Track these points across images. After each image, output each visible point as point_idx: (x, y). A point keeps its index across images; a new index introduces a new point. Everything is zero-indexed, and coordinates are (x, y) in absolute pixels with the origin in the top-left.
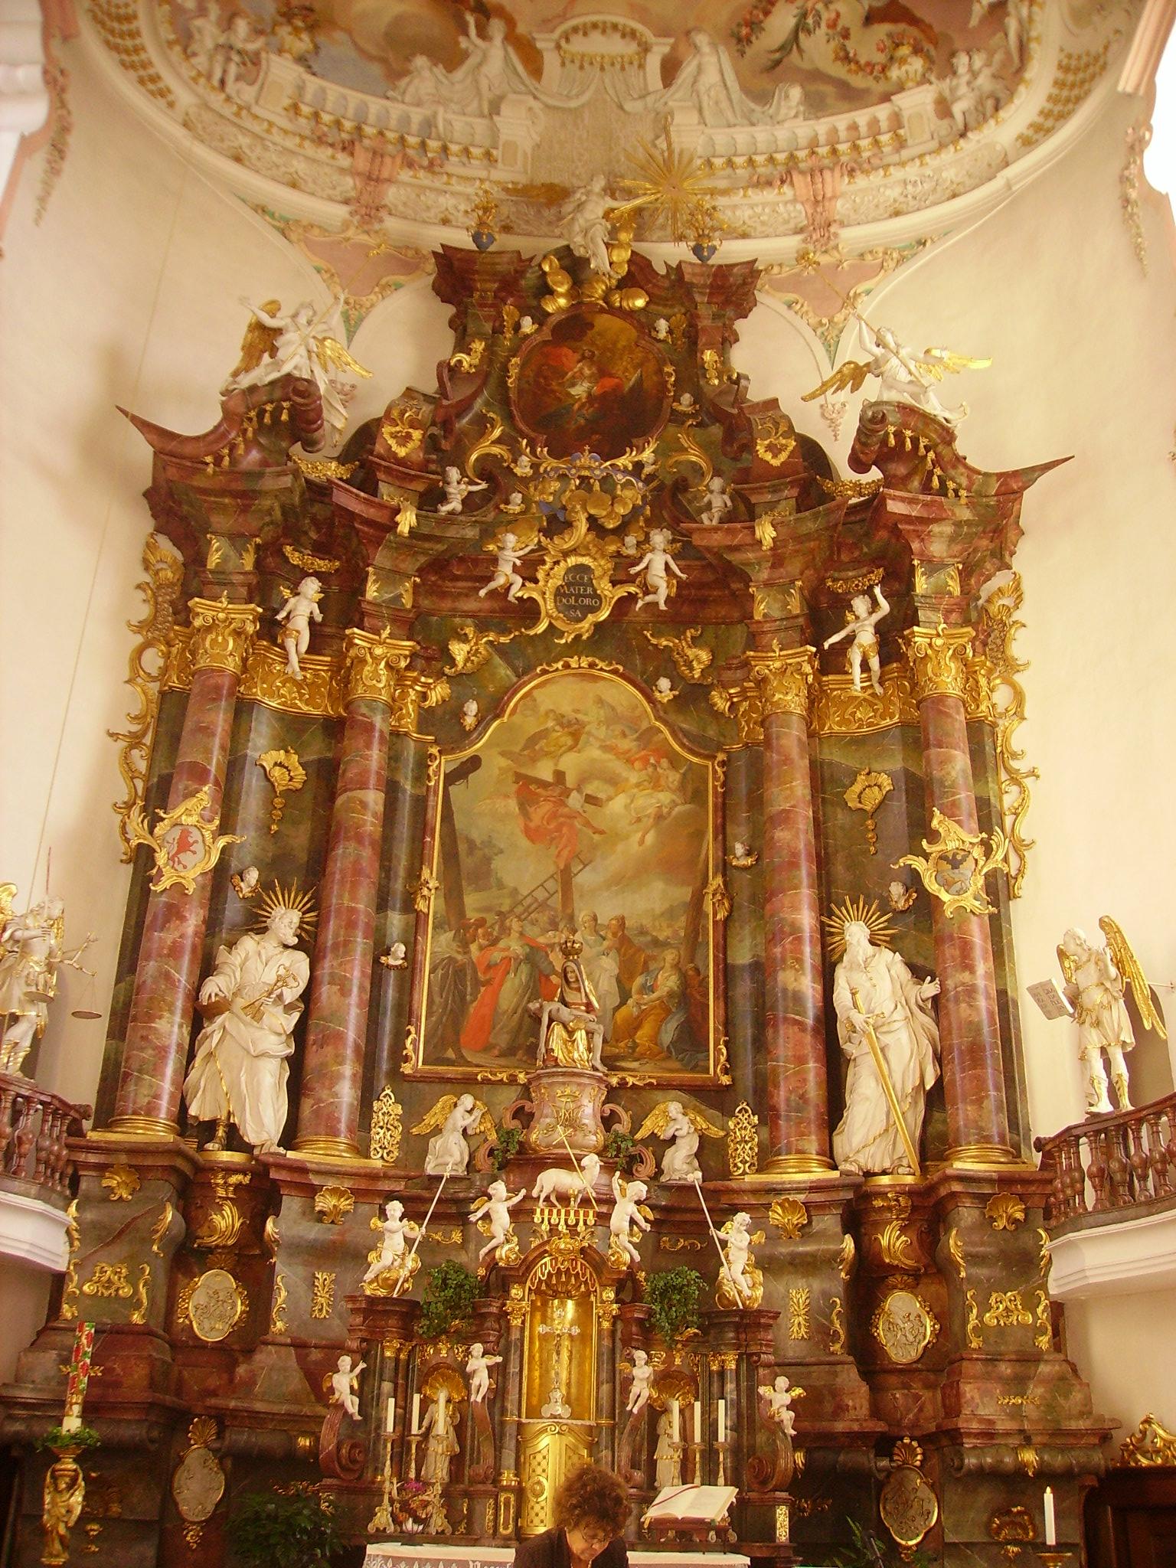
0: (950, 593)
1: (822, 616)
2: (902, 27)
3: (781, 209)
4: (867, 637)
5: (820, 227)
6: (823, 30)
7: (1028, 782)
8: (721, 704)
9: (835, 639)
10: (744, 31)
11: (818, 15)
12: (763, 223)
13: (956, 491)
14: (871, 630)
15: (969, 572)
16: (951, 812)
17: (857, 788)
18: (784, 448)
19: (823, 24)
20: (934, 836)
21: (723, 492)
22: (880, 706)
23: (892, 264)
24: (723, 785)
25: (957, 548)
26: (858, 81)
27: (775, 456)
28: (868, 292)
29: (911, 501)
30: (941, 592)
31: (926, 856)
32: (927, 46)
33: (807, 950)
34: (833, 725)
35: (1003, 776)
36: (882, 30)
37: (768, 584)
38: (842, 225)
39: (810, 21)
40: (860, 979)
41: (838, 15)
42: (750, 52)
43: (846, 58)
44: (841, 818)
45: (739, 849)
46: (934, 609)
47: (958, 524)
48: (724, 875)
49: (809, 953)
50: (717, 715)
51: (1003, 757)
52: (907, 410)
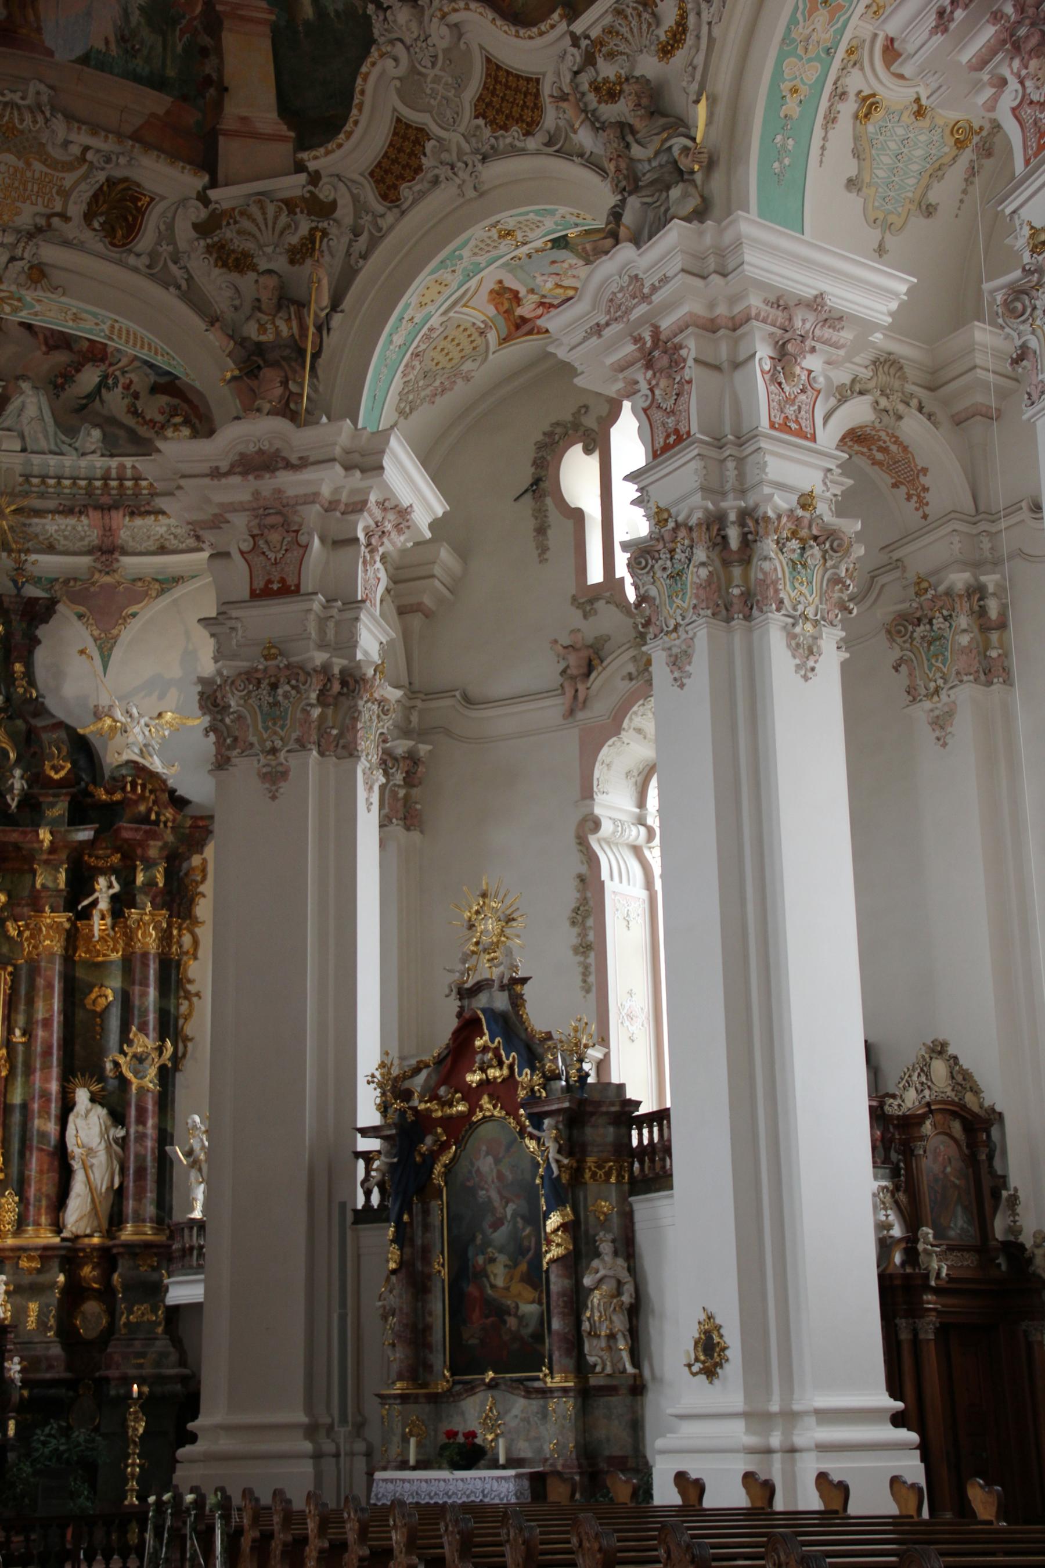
0: (156, 884)
1: (81, 884)
2: (176, 401)
3: (80, 528)
4: (103, 905)
5: (107, 551)
6: (120, 389)
7: (195, 999)
8: (13, 933)
9: (85, 903)
10: (60, 381)
11: (116, 378)
12: (66, 538)
13: (165, 823)
14: (108, 900)
15: (174, 860)
16: (143, 1028)
17: (93, 996)
18: (63, 768)
19: (120, 386)
20: (130, 1043)
21: (22, 777)
22: (111, 944)
23: (154, 594)
24: (10, 988)
25: (165, 853)
26: (143, 431)
27: (56, 773)
28: (134, 615)
29: (137, 830)
30: (151, 883)
31: (125, 1055)
32: (195, 421)
33: (53, 1105)
34: (81, 954)
35: (182, 994)
36: (163, 400)
37: (47, 862)
38: (125, 552)
39: (110, 381)
40: (80, 1122)
41: (131, 382)
42: (63, 396)
43: (134, 412)
44: (80, 1015)
45: (18, 1032)
46: (146, 894)
47: (166, 844)
48: (7, 1048)
49: (54, 1108)
50: (9, 939)
51: (181, 983)
52: (139, 769)
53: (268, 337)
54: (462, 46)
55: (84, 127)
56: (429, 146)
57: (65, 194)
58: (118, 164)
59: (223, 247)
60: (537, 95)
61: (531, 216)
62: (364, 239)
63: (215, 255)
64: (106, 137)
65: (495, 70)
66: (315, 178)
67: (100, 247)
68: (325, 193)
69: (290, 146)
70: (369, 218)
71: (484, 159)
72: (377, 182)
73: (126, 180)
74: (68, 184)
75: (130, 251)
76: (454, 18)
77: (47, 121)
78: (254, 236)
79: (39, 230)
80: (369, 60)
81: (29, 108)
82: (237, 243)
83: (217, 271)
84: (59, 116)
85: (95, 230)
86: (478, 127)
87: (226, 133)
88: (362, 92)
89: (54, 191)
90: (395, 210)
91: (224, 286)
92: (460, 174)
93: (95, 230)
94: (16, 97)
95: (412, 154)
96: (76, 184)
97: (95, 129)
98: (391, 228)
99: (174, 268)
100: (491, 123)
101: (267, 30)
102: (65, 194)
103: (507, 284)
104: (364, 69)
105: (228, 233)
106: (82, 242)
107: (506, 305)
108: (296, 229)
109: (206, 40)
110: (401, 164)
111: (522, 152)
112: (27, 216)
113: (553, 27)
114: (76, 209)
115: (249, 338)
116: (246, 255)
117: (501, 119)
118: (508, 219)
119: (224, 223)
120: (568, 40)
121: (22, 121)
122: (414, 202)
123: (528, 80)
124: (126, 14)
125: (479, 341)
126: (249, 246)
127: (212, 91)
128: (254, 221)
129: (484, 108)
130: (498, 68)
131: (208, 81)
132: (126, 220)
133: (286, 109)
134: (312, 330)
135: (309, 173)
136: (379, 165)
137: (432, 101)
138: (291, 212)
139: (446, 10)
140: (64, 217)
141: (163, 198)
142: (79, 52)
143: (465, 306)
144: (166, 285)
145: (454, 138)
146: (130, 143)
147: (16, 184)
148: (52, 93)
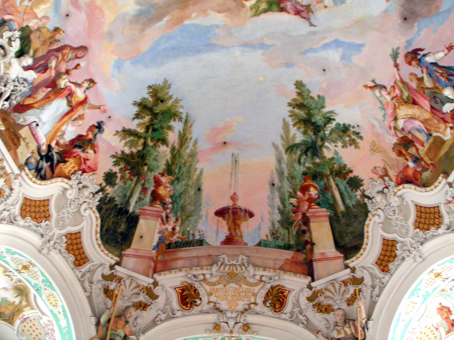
53: (342, 335)
54: (405, 203)
55: (260, 268)
56: (398, 246)
57: (255, 295)
58: (275, 280)
59: (319, 304)
60: (439, 212)
61: (448, 264)
62: (377, 289)
63: (317, 308)
64: (269, 270)
65: (420, 209)
66: (353, 270)
67: (270, 313)
68: (358, 275)
69: (342, 260)
70: (378, 280)
71: (422, 244)
72: (379, 266)
73: (278, 285)
74: (256, 291)
75: (283, 313)
76: (399, 193)
77: (246, 268)
78: (332, 298)
79: (246, 310)
80: (369, 219)
81: (240, 265)
82: (325, 302)
83: (318, 314)
84: (251, 265)
85: (268, 307)
86: (417, 232)
87: (316, 260)
88: (367, 232)
89: (251, 294)
90: (388, 274)
91: (321, 320)
92: (413, 252)
93: (268, 307)
94: (234, 262)
95: (392, 251)
96: (259, 290)
97: (265, 269)
98: (388, 282)
99: (301, 317)
100: (422, 229)
101: (327, 219)
102: (255, 295)
103: (444, 304)
104: (367, 223)
105: (321, 299)
106: (263, 312)
107: (445, 315)
108: (349, 291)
109: (304, 228)
110: (388, 256)
111: (438, 235)
112: (241, 306)
113: (440, 183)
114: (260, 300)
115: (334, 338)
116: (329, 306)
117: (426, 226)
118: (437, 267)
119: (319, 295)
120: (447, 186)
121: (237, 270)
122: (396, 269)
123: (434, 208)
124: (273, 224)
125: (437, 333)
126: (330, 302)
127: (309, 246)
128: (331, 292)
129: (419, 225)
130: (421, 207)
131: (307, 242)
132: (279, 301)
133: (338, 246)
134: (360, 329)
135: (351, 269)
136: (379, 259)
137: (397, 228)
138: (346, 285)
139: (395, 191)
140: (255, 304)
141: (294, 290)
142: (257, 242)
143: (427, 317)
144: (298, 324)
145: (408, 240)
146: (279, 271)
147: (236, 294)
148: (248, 258)
